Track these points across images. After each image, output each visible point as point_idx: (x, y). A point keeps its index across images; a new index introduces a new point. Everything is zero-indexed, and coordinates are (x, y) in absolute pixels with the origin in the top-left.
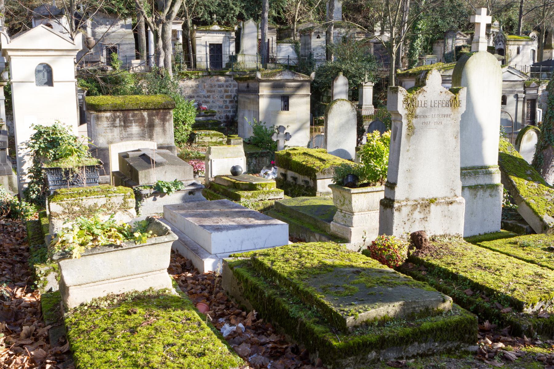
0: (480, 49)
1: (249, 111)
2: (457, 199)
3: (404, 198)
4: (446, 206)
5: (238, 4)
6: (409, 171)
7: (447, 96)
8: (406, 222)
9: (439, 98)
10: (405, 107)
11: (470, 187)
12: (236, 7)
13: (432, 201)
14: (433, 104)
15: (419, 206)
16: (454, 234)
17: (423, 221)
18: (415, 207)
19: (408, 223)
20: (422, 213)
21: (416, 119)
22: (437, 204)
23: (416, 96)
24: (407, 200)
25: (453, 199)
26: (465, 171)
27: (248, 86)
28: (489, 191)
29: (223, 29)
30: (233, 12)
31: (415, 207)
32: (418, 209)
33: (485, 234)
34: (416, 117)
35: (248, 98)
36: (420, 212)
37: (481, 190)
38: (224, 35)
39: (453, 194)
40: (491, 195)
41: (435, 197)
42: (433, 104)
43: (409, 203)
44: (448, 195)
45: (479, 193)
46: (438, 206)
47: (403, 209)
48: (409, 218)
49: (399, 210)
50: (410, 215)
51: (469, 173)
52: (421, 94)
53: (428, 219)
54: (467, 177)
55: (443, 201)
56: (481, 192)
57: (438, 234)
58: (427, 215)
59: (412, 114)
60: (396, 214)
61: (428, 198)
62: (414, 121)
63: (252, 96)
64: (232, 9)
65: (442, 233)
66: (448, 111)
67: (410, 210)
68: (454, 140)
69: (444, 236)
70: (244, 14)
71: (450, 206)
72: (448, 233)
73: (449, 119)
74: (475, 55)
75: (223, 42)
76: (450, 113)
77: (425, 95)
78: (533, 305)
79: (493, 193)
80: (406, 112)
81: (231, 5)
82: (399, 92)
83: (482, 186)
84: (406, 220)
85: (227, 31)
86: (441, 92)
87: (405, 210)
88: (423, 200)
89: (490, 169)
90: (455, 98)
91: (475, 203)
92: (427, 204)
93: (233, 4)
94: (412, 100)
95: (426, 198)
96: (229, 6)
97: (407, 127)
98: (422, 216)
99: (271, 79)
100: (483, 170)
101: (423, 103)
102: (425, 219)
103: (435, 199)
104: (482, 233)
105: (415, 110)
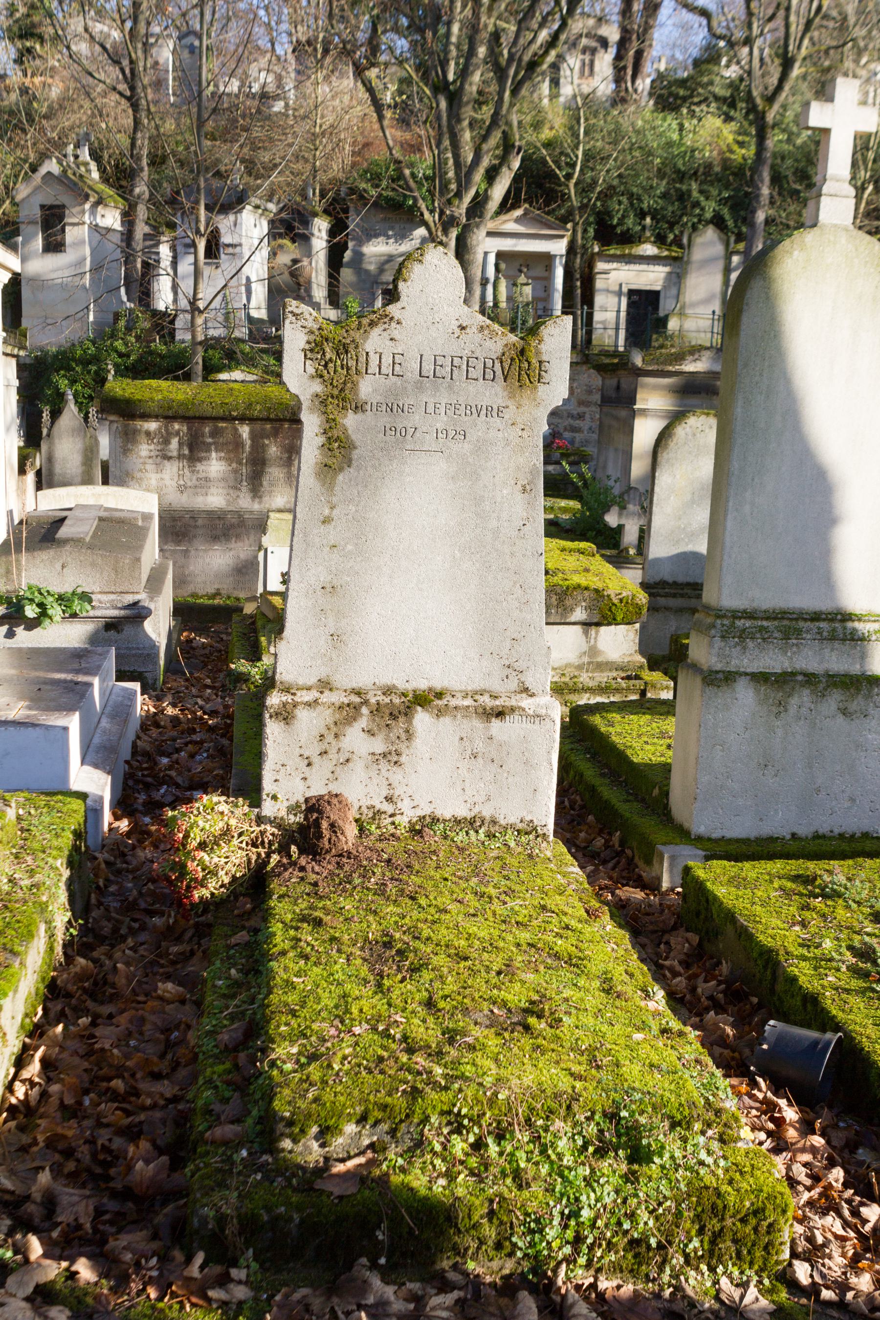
0: (824, 216)
1: (616, 450)
2: (526, 703)
3: (313, 681)
4: (477, 723)
5: (714, 192)
6: (331, 589)
7: (489, 344)
8: (316, 760)
9: (453, 348)
10: (311, 370)
11: (760, 678)
12: (707, 198)
13: (421, 700)
14: (428, 368)
15: (365, 710)
16: (512, 819)
17: (384, 765)
18: (348, 713)
19: (322, 768)
20: (380, 737)
21: (360, 416)
22: (440, 713)
23: (357, 335)
24: (325, 685)
25: (513, 703)
26: (748, 623)
27: (618, 388)
28: (834, 699)
29: (666, 253)
30: (697, 211)
31: (348, 713)
32: (363, 722)
33: (817, 836)
34: (359, 408)
35: (617, 418)
36: (370, 733)
37: (806, 692)
38: (667, 269)
39: (513, 684)
40: (844, 712)
41: (438, 686)
42: (428, 368)
43: (327, 697)
44: (496, 685)
45: (794, 701)
46: (446, 720)
47: (302, 714)
48: (324, 746)
49: (286, 715)
50: (330, 738)
51: (762, 629)
52: (376, 332)
53: (403, 759)
54: (750, 644)
55: (468, 702)
56: (802, 699)
57: (446, 812)
58: (402, 747)
59: (339, 396)
60: (273, 729)
61: (410, 687)
62: (350, 421)
63: (623, 413)
64: (697, 204)
65: (463, 812)
66: (493, 393)
67: (330, 721)
68: (519, 496)
69: (472, 824)
70: (727, 217)
71: (496, 723)
72: (487, 813)
73: (496, 421)
74: (808, 237)
75: (664, 287)
76: (501, 402)
77: (396, 334)
78: (325, 1133)
79: (853, 706)
80: (317, 387)
81: (695, 194)
82: (290, 318)
83: (810, 679)
84: (313, 751)
85: (675, 259)
86: (462, 328)
87: (309, 722)
88: (388, 691)
89: (850, 624)
90: (522, 352)
91: (780, 732)
92: (398, 709)
93: (701, 192)
94: (342, 349)
95: (401, 685)
96: (690, 196)
97: (321, 440)
98: (379, 745)
99: (671, 368)
100: (823, 624)
101: (387, 360)
102: (391, 757)
103: (439, 695)
104: (804, 831)
105: (355, 384)
